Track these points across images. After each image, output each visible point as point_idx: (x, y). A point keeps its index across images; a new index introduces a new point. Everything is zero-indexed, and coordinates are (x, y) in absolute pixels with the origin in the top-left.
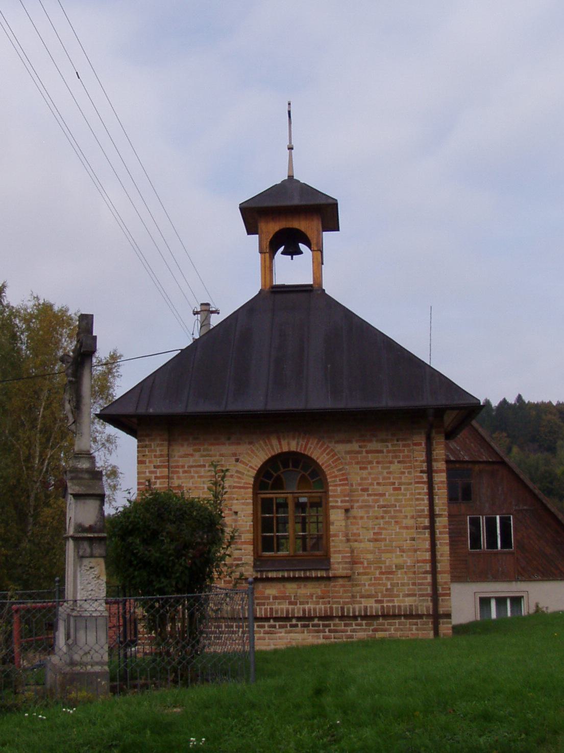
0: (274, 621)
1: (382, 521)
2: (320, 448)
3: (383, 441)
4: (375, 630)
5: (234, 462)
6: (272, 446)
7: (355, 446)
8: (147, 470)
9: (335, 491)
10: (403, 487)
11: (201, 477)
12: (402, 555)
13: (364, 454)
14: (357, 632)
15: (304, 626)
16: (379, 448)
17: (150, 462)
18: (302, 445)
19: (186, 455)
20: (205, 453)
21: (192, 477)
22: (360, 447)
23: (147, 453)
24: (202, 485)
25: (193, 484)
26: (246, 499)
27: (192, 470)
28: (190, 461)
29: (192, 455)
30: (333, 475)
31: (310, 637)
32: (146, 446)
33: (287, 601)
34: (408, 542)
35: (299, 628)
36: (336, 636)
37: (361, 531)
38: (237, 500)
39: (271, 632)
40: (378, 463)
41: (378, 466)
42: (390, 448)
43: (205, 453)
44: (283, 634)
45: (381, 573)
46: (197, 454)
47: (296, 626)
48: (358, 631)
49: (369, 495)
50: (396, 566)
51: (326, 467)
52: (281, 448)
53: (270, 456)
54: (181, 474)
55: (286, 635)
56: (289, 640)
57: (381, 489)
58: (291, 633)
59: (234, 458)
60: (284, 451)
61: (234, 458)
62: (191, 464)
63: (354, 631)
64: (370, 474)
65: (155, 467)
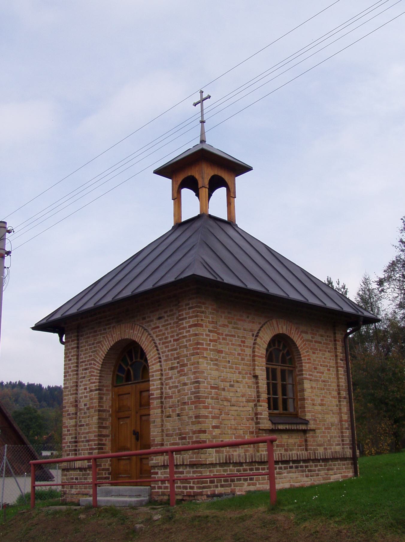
0: (282, 464)
1: (323, 392)
2: (297, 334)
3: (322, 336)
4: (328, 470)
5: (251, 336)
6: (274, 327)
7: (309, 337)
8: (204, 333)
9: (305, 367)
10: (331, 369)
11: (233, 344)
12: (333, 416)
13: (314, 343)
14: (320, 471)
15: (297, 467)
16: (320, 340)
17: (206, 326)
18: (289, 329)
19: (224, 326)
20: (235, 326)
21: (228, 344)
22: (312, 338)
23: (203, 318)
24: (234, 352)
25: (229, 349)
26: (263, 367)
27: (228, 338)
28: (226, 331)
29: (227, 326)
30: (304, 355)
31: (299, 476)
32: (202, 312)
33: (283, 448)
34: (335, 407)
35: (294, 470)
36: (312, 475)
37: (315, 398)
38: (258, 366)
39: (280, 473)
40: (320, 350)
41: (320, 353)
42: (324, 341)
43: (235, 326)
44: (285, 474)
45: (326, 429)
46: (230, 326)
47: (291, 467)
48: (320, 470)
49: (317, 372)
50: (331, 424)
51: (301, 348)
52: (279, 330)
53: (273, 335)
54: (221, 341)
55: (288, 474)
56: (289, 479)
57: (322, 369)
58: (290, 473)
59: (251, 333)
60: (280, 332)
61: (251, 333)
62: (227, 333)
63: (319, 470)
64: (317, 357)
65: (210, 331)
